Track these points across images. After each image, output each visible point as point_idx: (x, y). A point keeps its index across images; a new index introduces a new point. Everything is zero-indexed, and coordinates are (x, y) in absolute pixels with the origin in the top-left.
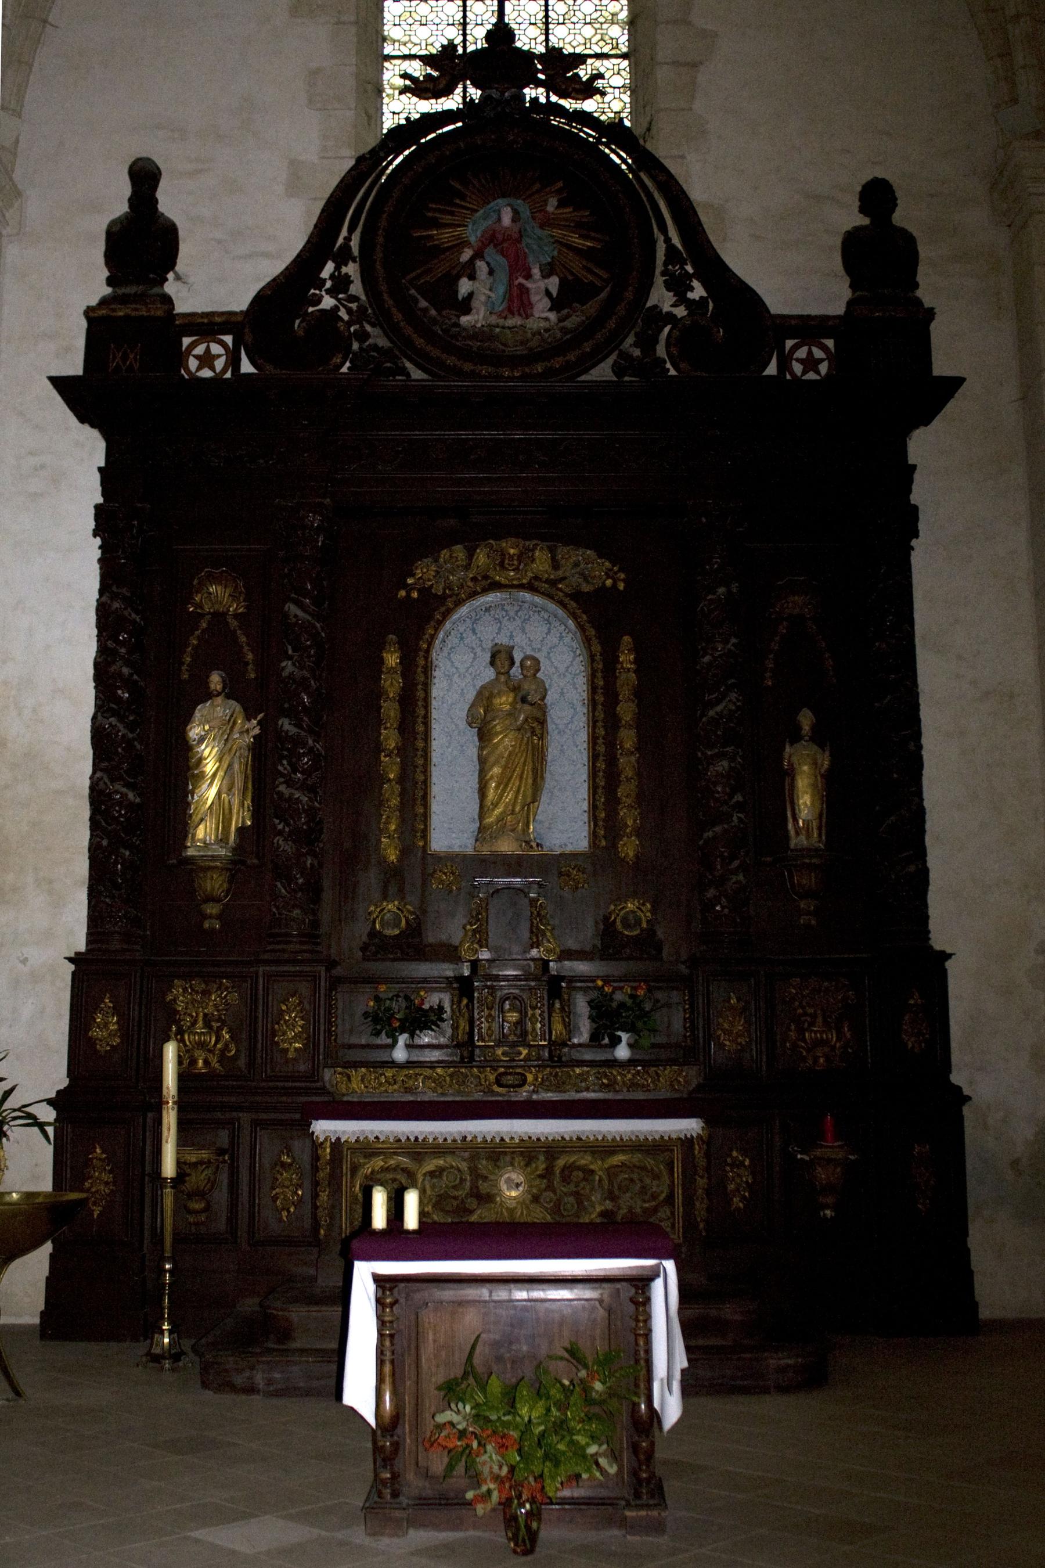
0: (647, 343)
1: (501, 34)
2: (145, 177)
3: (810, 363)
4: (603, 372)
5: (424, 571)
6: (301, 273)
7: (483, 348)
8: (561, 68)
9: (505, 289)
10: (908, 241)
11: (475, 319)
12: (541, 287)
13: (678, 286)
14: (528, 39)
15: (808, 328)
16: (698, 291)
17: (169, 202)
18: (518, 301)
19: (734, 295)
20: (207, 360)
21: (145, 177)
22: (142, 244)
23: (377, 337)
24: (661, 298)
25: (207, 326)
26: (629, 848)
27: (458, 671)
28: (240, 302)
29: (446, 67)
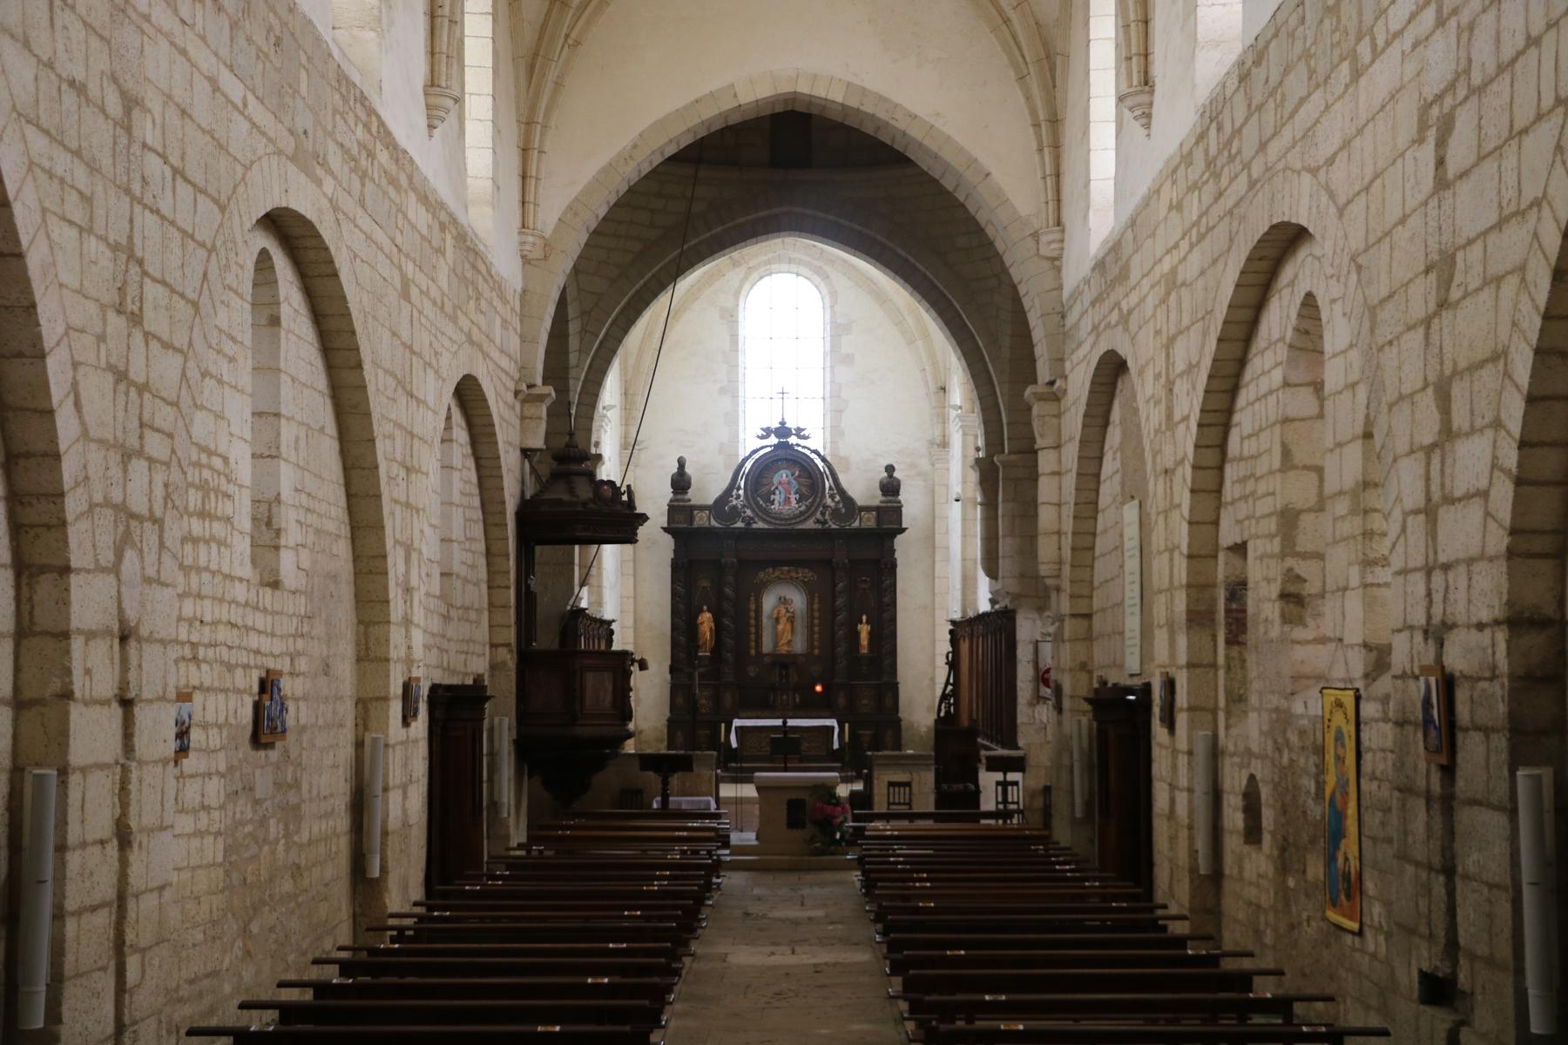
0: (823, 514)
1: (783, 423)
2: (681, 463)
3: (869, 521)
4: (810, 524)
5: (761, 575)
6: (728, 493)
7: (778, 517)
8: (799, 432)
9: (785, 500)
10: (898, 483)
11: (776, 507)
12: (793, 497)
13: (832, 497)
14: (791, 424)
15: (868, 509)
16: (838, 498)
17: (688, 470)
18: (787, 500)
19: (847, 500)
20: (701, 520)
21: (681, 463)
22: (680, 482)
23: (749, 512)
24: (829, 501)
25: (702, 508)
26: (816, 652)
27: (769, 602)
28: (710, 502)
29: (768, 432)
